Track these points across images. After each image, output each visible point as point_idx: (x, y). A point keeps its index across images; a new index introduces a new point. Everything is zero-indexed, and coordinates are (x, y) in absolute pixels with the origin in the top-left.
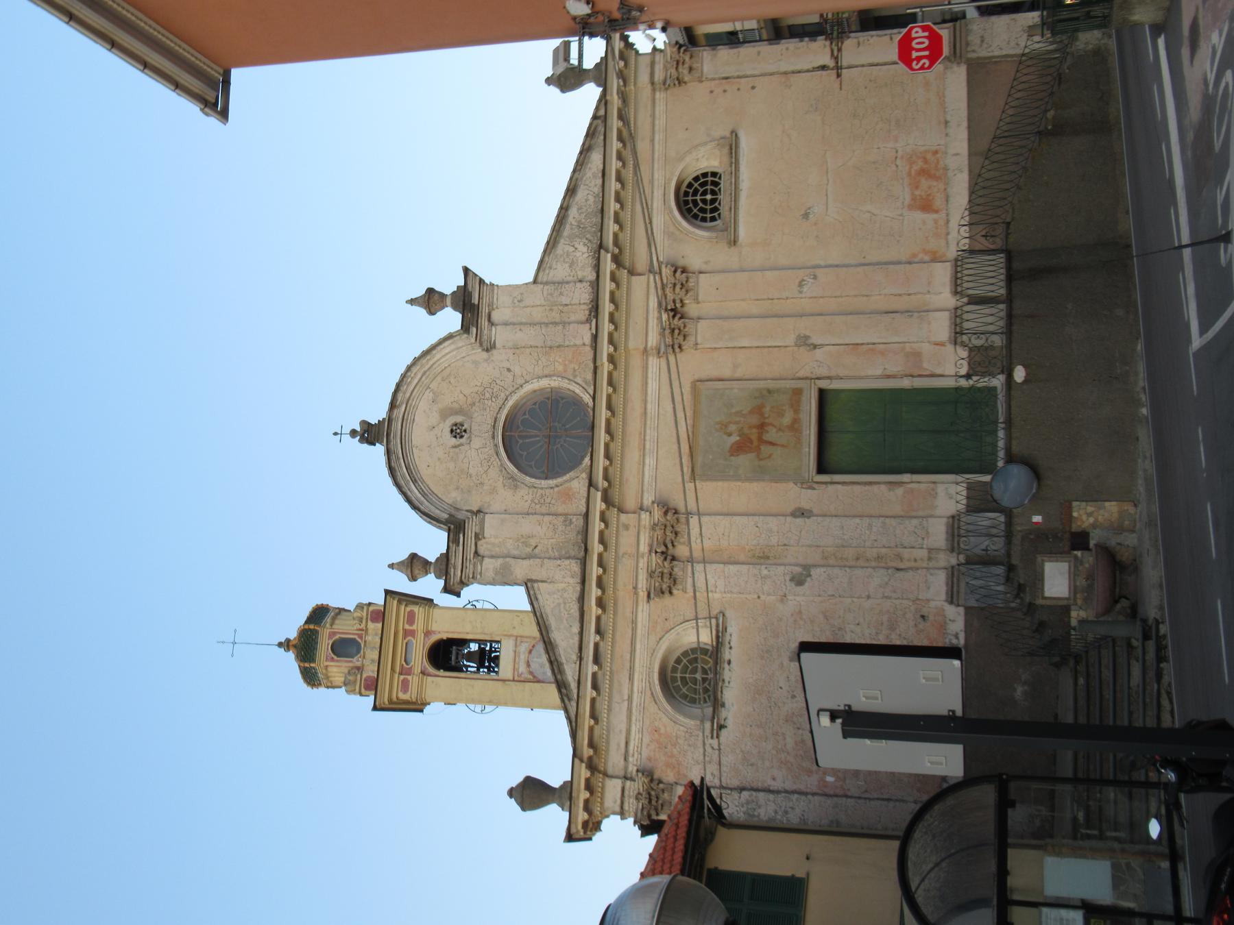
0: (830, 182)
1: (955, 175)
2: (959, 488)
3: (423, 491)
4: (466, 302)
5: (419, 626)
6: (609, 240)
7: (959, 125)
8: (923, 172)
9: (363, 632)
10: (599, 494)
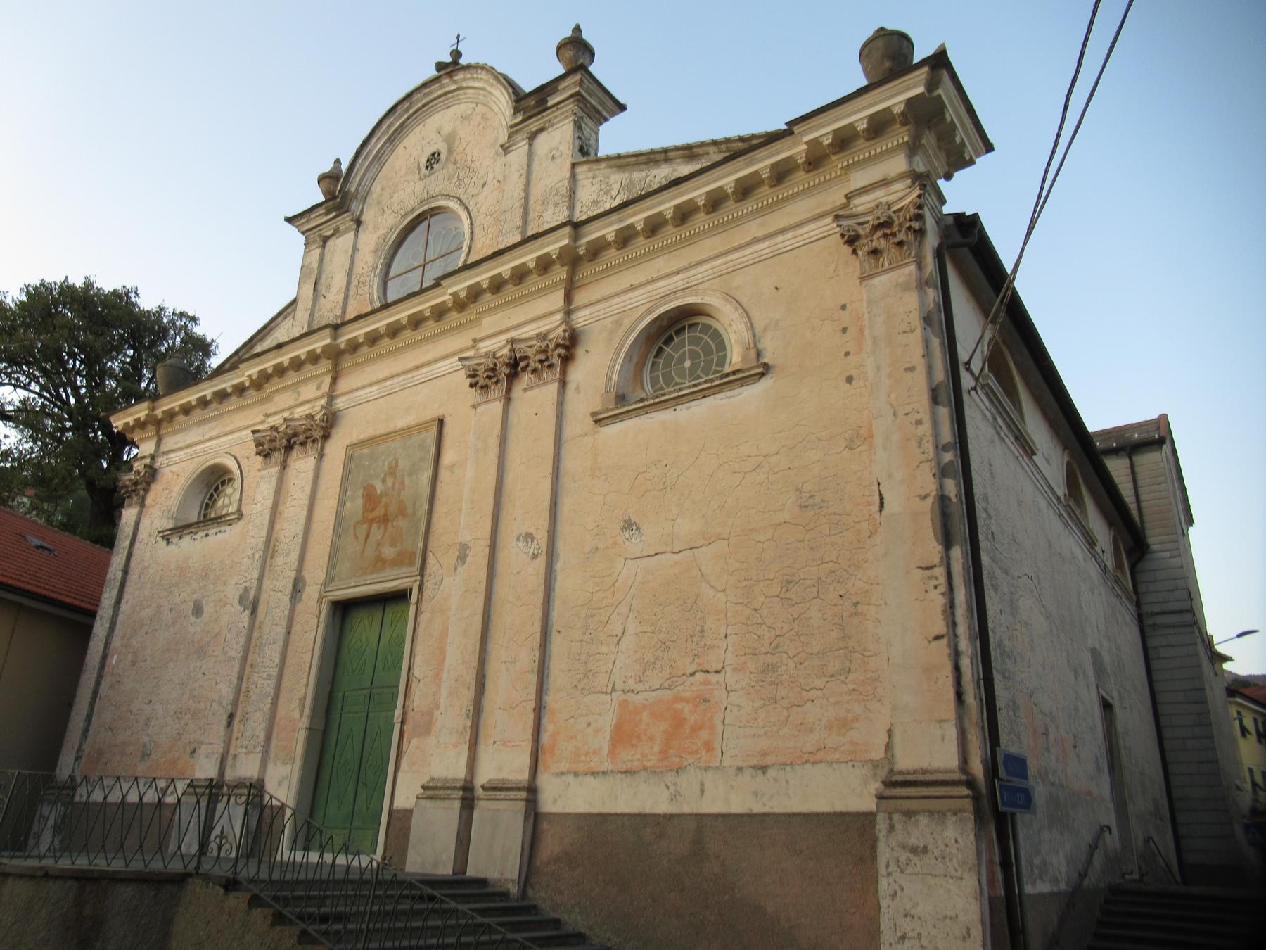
0: (678, 557)
1: (668, 787)
3: (382, 155)
4: (545, 91)
6: (592, 234)
7: (756, 794)
8: (678, 721)
10: (328, 341)
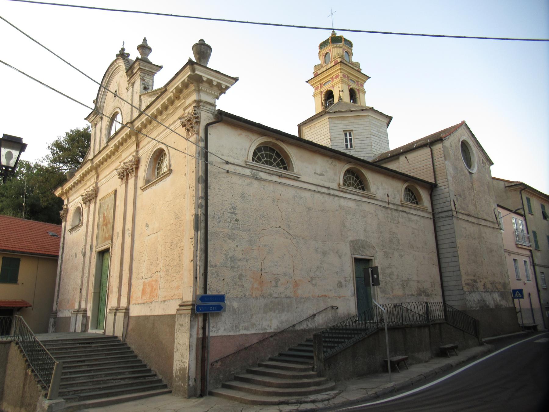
10: (91, 165)
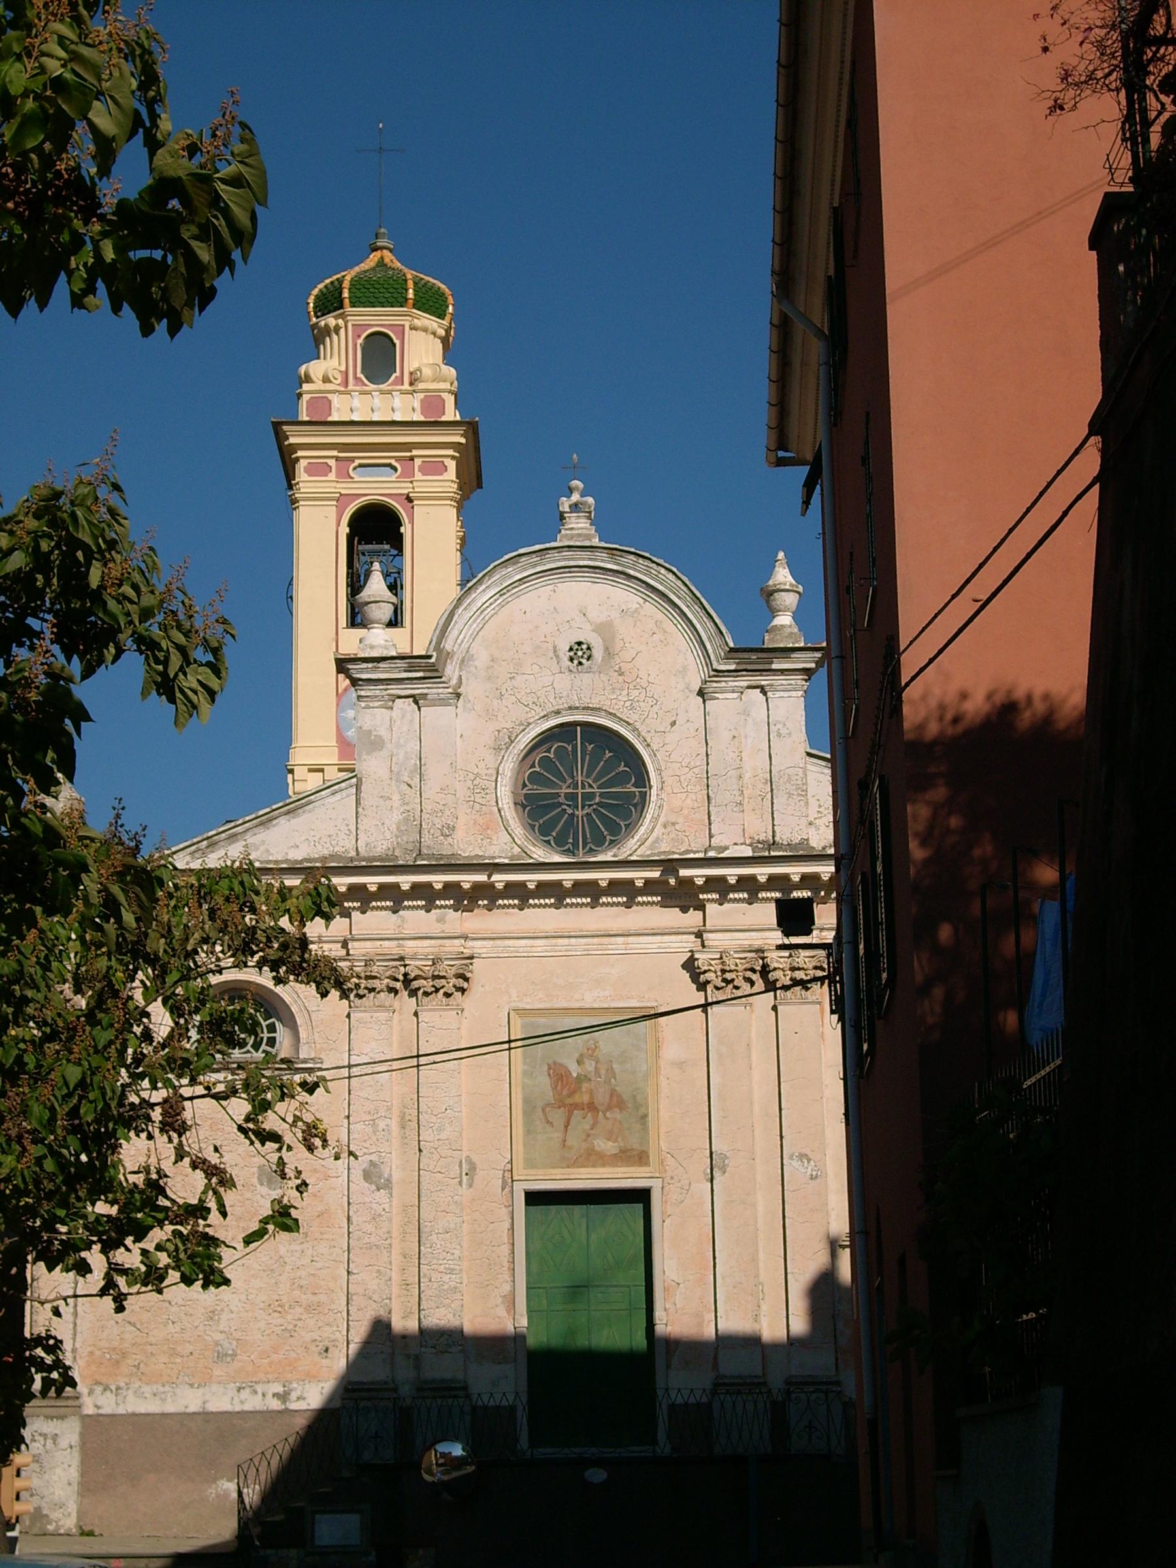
2: (511, 1398)
5: (422, 484)
9: (406, 386)
